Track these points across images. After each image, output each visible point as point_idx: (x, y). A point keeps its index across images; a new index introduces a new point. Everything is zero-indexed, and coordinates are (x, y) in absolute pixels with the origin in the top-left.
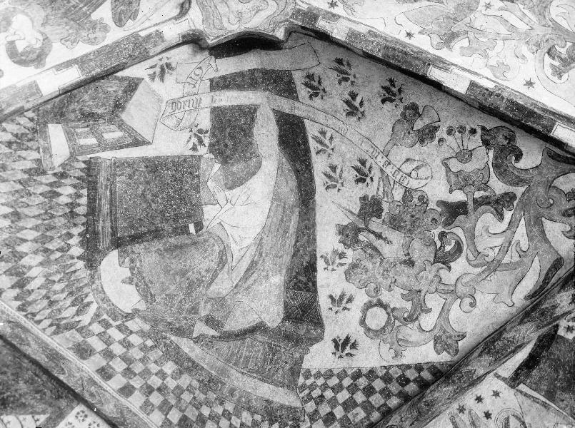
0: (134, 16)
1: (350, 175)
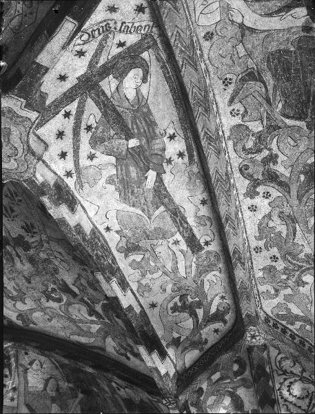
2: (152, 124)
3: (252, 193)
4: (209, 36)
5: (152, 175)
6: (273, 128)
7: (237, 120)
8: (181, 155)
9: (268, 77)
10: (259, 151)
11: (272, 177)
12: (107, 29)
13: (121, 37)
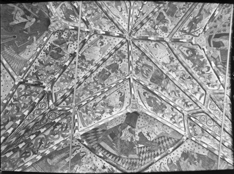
0: (202, 56)
1: (224, 28)
2: (190, 23)
5: (197, 18)
6: (180, 9)
8: (192, 16)
9: (175, 15)
10: (184, 8)
12: (181, 36)
13: (181, 34)
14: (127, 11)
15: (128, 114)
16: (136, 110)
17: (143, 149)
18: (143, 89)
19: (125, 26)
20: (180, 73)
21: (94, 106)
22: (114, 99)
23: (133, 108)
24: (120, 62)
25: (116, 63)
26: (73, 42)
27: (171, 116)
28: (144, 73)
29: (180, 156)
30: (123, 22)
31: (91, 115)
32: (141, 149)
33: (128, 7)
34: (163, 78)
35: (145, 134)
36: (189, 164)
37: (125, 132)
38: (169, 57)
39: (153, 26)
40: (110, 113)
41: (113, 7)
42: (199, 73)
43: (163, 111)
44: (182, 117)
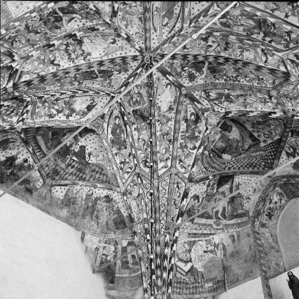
2: (221, 93)
3: (239, 81)
4: (206, 82)
5: (231, 97)
7: (223, 80)
9: (215, 74)
11: (236, 77)
12: (201, 97)
14: (171, 31)
15: (86, 127)
16: (96, 130)
17: (74, 163)
18: (118, 113)
19: (154, 43)
20: (166, 129)
21: (55, 100)
22: (80, 104)
23: (94, 126)
24: (118, 72)
25: (113, 72)
26: (82, 18)
27: (123, 160)
28: (133, 100)
29: (103, 196)
30: (156, 38)
31: (47, 108)
32: (73, 162)
33: (176, 29)
34: (146, 121)
35: (87, 152)
36: (104, 209)
37: (69, 135)
38: (171, 106)
39: (183, 66)
40: (68, 116)
41: (160, 15)
42: (183, 143)
43: (120, 149)
44: (133, 169)
